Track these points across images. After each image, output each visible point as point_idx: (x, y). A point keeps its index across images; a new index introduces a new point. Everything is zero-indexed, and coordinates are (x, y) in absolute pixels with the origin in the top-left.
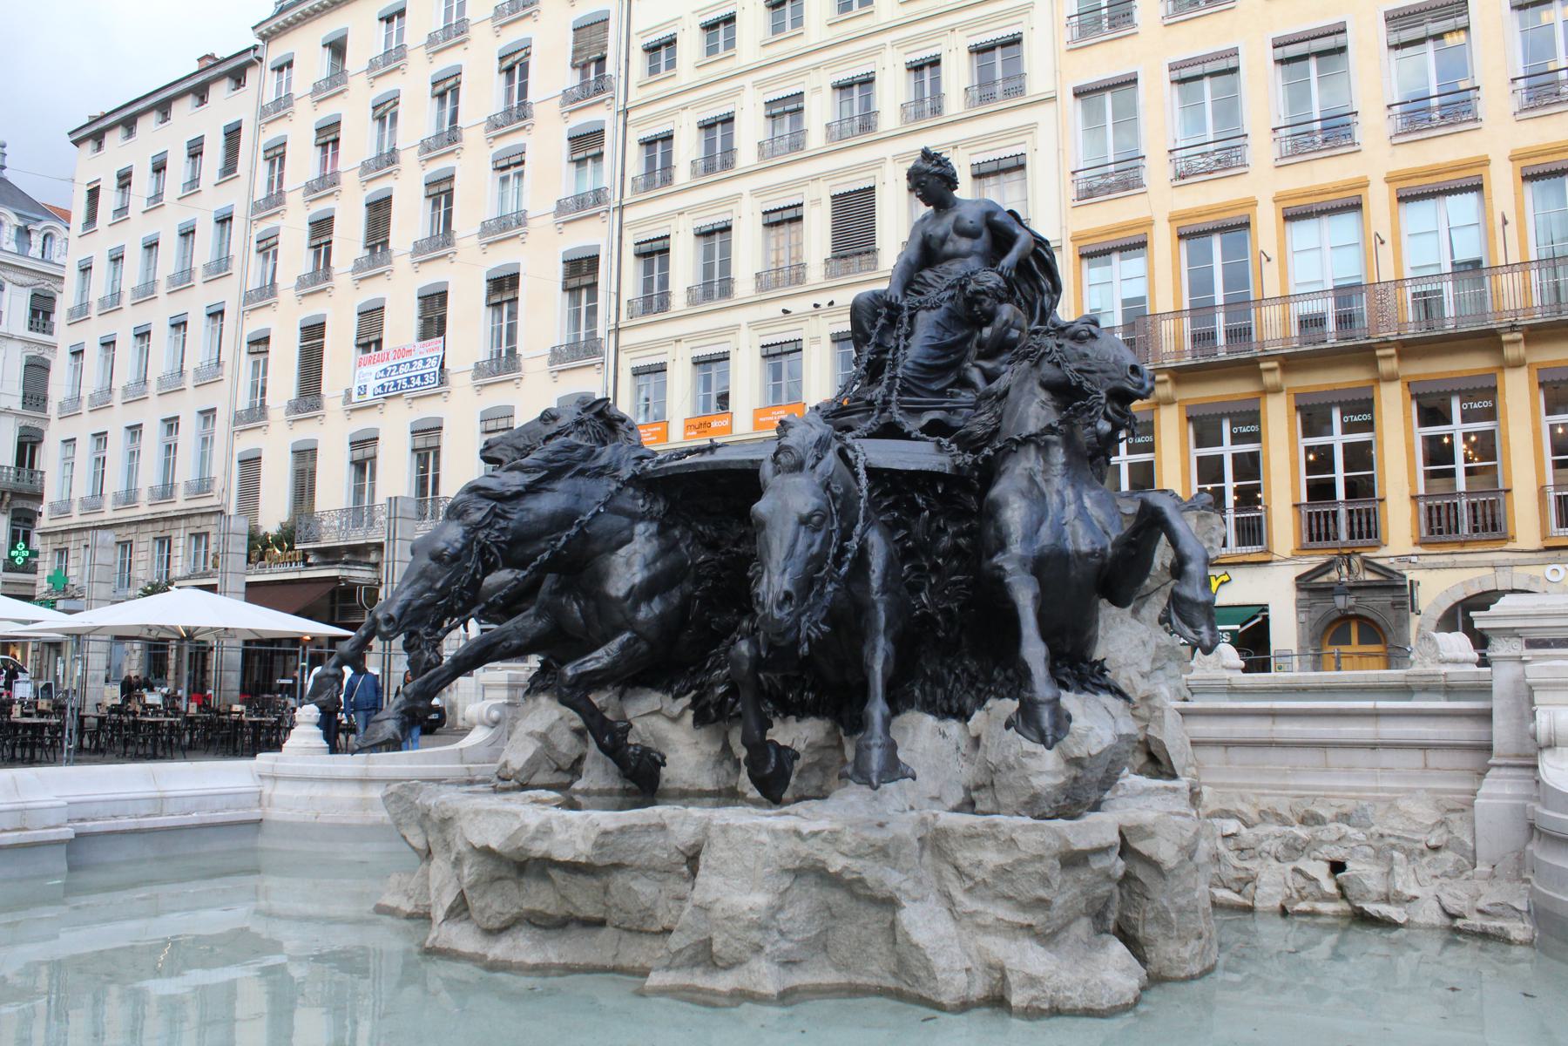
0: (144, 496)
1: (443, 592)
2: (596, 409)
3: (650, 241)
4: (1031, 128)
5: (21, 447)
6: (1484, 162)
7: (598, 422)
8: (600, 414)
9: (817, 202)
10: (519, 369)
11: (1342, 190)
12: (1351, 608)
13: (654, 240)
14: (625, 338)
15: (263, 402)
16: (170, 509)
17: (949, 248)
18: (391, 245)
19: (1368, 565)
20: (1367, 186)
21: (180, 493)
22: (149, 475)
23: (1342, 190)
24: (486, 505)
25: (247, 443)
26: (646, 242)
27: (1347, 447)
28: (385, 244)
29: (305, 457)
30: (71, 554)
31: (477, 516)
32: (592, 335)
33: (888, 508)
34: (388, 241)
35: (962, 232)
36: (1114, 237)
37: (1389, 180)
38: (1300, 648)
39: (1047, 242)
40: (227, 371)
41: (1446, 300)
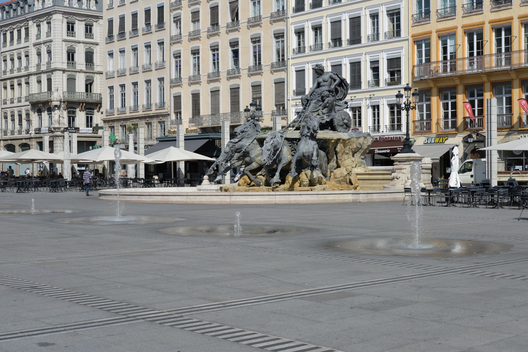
0: (140, 108)
1: (226, 157)
2: (253, 123)
5: (87, 86)
6: (512, 18)
8: (254, 123)
10: (262, 70)
15: (180, 76)
16: (150, 113)
17: (322, 84)
18: (220, 24)
20: (484, 24)
21: (153, 108)
22: (143, 101)
24: (232, 144)
25: (176, 91)
28: (217, 24)
29: (196, 97)
30: (115, 128)
31: (231, 146)
33: (290, 143)
34: (218, 23)
35: (324, 81)
36: (422, 36)
39: (345, 79)
40: (167, 65)
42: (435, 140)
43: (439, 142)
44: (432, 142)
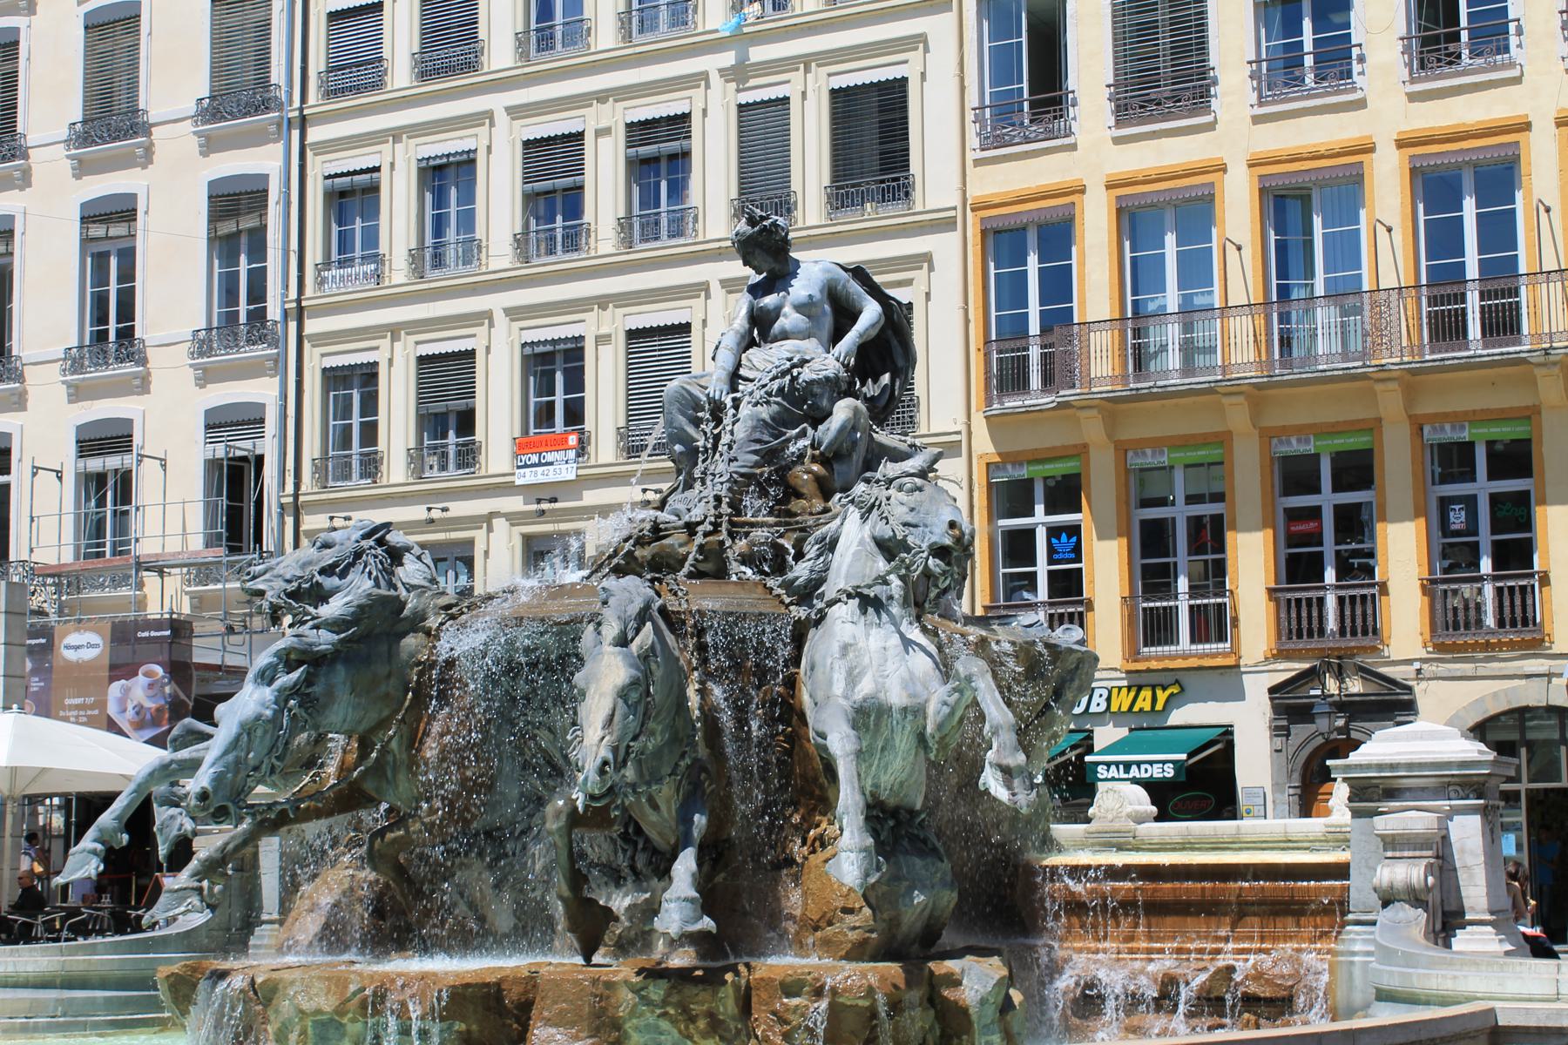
3: (349, 174)
4: (919, 41)
7: (379, 551)
9: (606, 132)
11: (1338, 155)
12: (1340, 730)
13: (355, 173)
14: (312, 326)
19: (1367, 673)
23: (1338, 155)
26: (342, 175)
27: (1339, 510)
32: (258, 316)
37: (1401, 144)
38: (1276, 786)
41: (1470, 311)
42: (1109, 700)
43: (1136, 709)
44: (1093, 709)
